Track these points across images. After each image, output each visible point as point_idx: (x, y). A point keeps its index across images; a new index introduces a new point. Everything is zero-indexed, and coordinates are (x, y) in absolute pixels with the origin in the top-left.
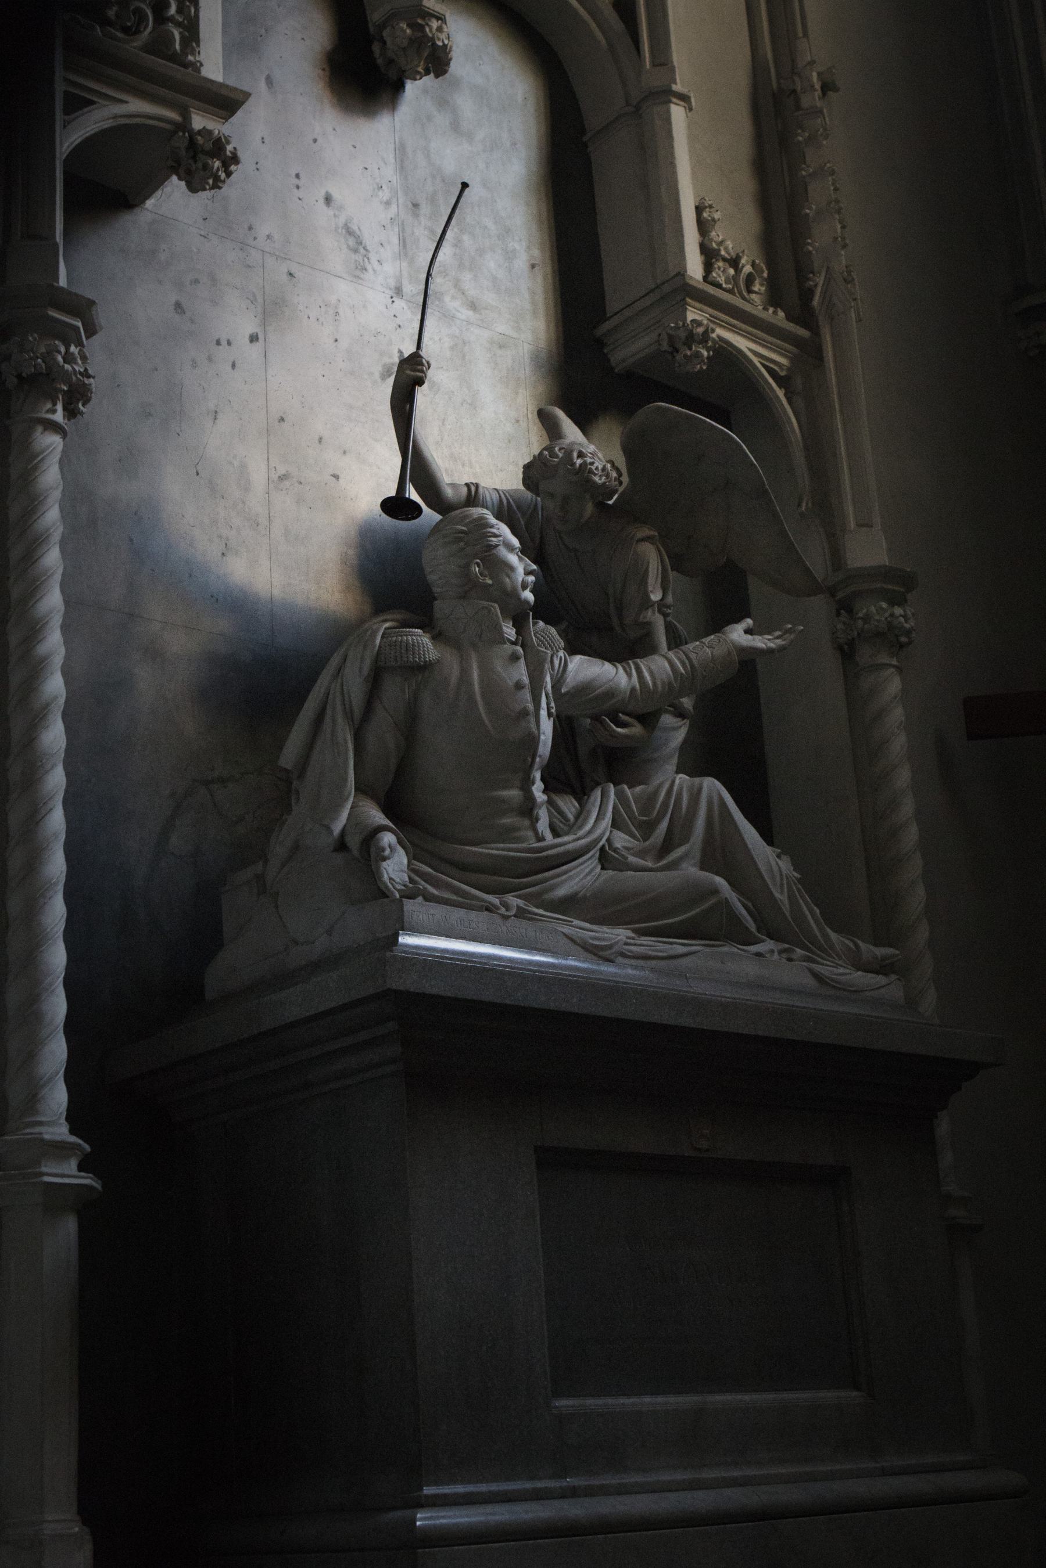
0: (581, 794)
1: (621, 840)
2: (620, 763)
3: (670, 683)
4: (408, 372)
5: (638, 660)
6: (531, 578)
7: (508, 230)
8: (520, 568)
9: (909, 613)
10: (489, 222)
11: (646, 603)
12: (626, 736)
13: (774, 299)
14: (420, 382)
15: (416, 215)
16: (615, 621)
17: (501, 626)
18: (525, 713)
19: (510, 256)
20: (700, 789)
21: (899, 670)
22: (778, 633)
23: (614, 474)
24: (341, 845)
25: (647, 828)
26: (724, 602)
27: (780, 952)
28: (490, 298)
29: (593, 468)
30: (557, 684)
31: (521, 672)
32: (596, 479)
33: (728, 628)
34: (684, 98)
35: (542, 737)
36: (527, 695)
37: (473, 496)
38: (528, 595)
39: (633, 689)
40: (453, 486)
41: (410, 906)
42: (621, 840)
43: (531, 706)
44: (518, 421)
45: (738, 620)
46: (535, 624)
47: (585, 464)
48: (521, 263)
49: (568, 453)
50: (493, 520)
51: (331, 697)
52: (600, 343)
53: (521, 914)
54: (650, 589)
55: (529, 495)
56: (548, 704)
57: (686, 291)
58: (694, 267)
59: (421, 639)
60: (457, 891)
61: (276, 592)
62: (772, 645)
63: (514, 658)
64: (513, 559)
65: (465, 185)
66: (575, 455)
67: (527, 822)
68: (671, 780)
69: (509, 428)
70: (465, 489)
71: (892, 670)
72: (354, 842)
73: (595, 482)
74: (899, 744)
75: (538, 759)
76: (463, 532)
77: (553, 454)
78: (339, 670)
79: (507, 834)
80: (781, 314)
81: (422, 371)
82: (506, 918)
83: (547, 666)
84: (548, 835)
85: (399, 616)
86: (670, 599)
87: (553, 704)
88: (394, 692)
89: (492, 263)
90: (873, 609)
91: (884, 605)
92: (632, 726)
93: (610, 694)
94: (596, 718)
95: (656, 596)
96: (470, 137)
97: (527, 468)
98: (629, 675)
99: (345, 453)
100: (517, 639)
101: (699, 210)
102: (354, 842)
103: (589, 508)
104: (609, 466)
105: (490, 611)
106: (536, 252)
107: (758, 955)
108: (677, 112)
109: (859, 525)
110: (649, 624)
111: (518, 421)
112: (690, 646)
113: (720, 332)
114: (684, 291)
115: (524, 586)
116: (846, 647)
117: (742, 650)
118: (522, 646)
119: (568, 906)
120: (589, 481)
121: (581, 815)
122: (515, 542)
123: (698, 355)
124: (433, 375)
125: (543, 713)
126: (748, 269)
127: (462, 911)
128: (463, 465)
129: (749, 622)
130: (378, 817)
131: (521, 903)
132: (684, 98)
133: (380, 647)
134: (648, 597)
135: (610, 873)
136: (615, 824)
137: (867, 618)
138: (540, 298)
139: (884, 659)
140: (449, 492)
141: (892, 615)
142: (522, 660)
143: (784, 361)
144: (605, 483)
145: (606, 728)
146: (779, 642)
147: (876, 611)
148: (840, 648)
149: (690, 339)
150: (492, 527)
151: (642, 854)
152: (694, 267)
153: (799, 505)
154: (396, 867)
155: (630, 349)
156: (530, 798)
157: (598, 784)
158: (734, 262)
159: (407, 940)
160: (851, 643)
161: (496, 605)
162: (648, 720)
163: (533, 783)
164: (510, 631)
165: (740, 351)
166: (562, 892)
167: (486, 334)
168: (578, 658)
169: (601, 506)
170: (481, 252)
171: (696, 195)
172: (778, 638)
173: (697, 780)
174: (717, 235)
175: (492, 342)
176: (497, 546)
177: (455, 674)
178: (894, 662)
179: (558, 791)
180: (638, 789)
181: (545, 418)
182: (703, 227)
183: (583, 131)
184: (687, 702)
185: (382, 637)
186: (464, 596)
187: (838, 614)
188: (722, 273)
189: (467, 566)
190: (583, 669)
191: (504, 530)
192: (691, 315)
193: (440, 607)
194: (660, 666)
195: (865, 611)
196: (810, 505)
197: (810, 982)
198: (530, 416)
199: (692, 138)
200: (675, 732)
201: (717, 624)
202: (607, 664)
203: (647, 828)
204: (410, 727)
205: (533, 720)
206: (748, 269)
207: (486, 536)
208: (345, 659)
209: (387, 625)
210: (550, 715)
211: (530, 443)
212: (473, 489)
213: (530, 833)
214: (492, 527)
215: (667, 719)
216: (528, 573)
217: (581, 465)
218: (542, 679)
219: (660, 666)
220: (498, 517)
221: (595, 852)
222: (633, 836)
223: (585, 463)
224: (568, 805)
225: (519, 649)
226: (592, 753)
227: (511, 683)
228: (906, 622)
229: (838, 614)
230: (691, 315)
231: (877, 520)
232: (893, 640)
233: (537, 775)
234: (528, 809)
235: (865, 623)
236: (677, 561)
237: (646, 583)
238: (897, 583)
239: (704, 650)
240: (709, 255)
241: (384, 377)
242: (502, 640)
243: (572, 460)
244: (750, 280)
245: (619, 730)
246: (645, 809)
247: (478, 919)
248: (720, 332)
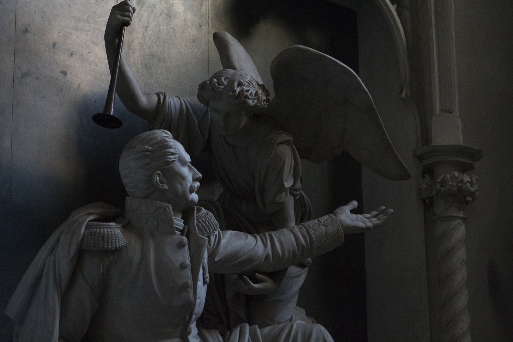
3: (294, 252)
4: (119, 17)
5: (273, 233)
6: (197, 184)
9: (474, 179)
11: (281, 188)
12: (260, 289)
14: (127, 24)
17: (173, 222)
18: (185, 286)
20: (311, 334)
21: (464, 220)
22: (375, 213)
23: (264, 97)
29: (248, 94)
32: (250, 102)
33: (338, 210)
35: (198, 301)
36: (188, 273)
38: (195, 197)
39: (267, 256)
43: (190, 282)
44: (201, 26)
45: (346, 203)
46: (199, 211)
47: (242, 91)
49: (231, 82)
51: (46, 267)
54: (285, 178)
56: (204, 275)
62: (369, 224)
63: (181, 245)
66: (236, 84)
69: (194, 32)
70: (156, 98)
71: (459, 221)
73: (249, 105)
74: (461, 276)
75: (194, 317)
76: (148, 151)
77: (220, 83)
78: (53, 250)
81: (129, 16)
85: (98, 211)
86: (299, 185)
87: (207, 275)
88: (92, 268)
90: (448, 176)
91: (456, 174)
92: (266, 282)
93: (250, 260)
94: (240, 276)
95: (288, 184)
97: (202, 86)
98: (265, 245)
99: (72, 55)
100: (184, 228)
103: (244, 121)
104: (260, 92)
105: (165, 210)
109: (442, 110)
110: (283, 203)
111: (201, 26)
115: (191, 191)
116: (427, 201)
118: (187, 236)
120: (245, 104)
122: (187, 157)
124: (136, 20)
128: (159, 61)
129: (355, 203)
133: (84, 235)
134: (283, 185)
137: (443, 183)
139: (454, 212)
140: (143, 100)
141: (462, 181)
142: (187, 247)
144: (256, 105)
146: (375, 221)
147: (450, 177)
148: (424, 200)
150: (171, 147)
153: (401, 92)
157: (239, 321)
160: (431, 198)
161: (170, 206)
162: (277, 275)
163: (189, 334)
164: (179, 222)
168: (229, 234)
172: (375, 216)
176: (173, 161)
177: (137, 254)
178: (461, 215)
180: (267, 330)
181: (219, 41)
185: (86, 228)
187: (423, 177)
189: (151, 176)
191: (179, 148)
194: (288, 238)
195: (442, 177)
196: (409, 93)
198: (210, 22)
200: (298, 278)
201: (333, 206)
202: (249, 236)
204: (102, 294)
205: (191, 291)
207: (166, 154)
208: (58, 241)
209: (91, 218)
210: (204, 282)
212: (162, 98)
214: (171, 147)
216: (195, 180)
217: (239, 92)
219: (288, 238)
223: (242, 90)
225: (185, 239)
227: (177, 264)
228: (471, 186)
229: (423, 177)
231: (456, 108)
232: (461, 198)
235: (442, 186)
237: (282, 175)
238: (466, 158)
239: (320, 226)
242: (171, 230)
243: (234, 88)
245: (255, 285)
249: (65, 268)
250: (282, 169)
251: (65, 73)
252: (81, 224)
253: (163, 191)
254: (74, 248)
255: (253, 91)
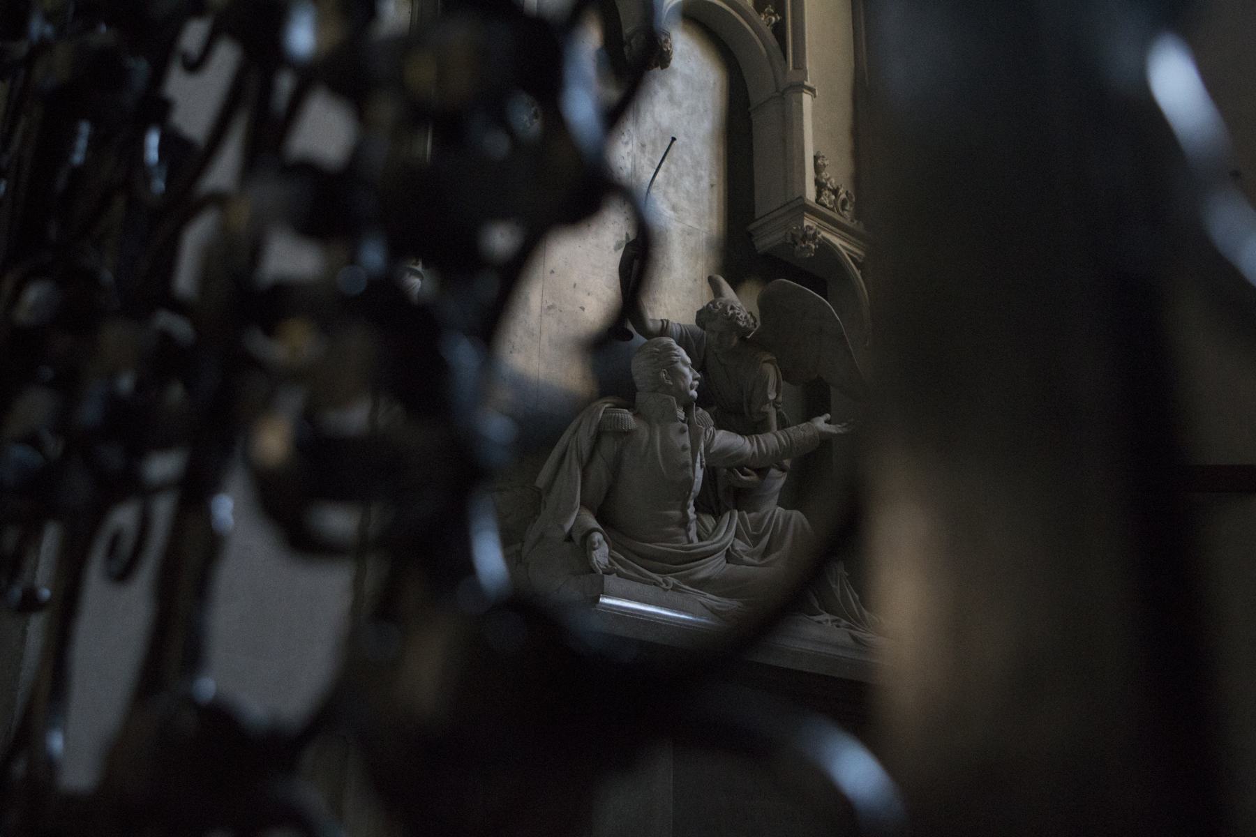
0: (717, 515)
1: (740, 546)
2: (743, 498)
6: (696, 383)
7: (698, 163)
8: (690, 375)
10: (687, 158)
11: (766, 400)
13: (858, 215)
15: (643, 152)
16: (746, 409)
18: (686, 465)
19: (698, 179)
24: (569, 538)
25: (756, 539)
26: (815, 403)
27: (833, 621)
28: (684, 204)
30: (707, 448)
31: (686, 440)
33: (815, 419)
34: (812, 90)
36: (689, 452)
37: (664, 330)
38: (694, 393)
40: (654, 320)
41: (610, 581)
42: (740, 546)
43: (690, 462)
45: (820, 414)
48: (705, 183)
49: (725, 306)
50: (676, 346)
52: (750, 235)
53: (675, 588)
55: (699, 329)
57: (804, 208)
58: (810, 193)
59: (627, 416)
60: (637, 571)
61: (541, 377)
63: (682, 431)
64: (686, 370)
65: (674, 139)
67: (683, 531)
68: (772, 510)
69: (690, 284)
72: (577, 536)
77: (715, 307)
78: (575, 431)
79: (669, 538)
80: (861, 224)
82: (666, 590)
83: (703, 436)
84: (695, 539)
88: (609, 447)
89: (687, 183)
93: (739, 455)
94: (730, 470)
95: (772, 397)
96: (679, 105)
97: (699, 313)
101: (816, 158)
102: (577, 536)
103: (735, 340)
106: (715, 177)
107: (819, 622)
108: (807, 98)
112: (791, 429)
113: (823, 233)
114: (802, 208)
115: (692, 387)
117: (822, 433)
119: (704, 584)
121: (716, 528)
122: (688, 360)
123: (809, 247)
125: (698, 465)
126: (843, 196)
127: (639, 585)
129: (828, 416)
130: (593, 523)
131: (676, 581)
132: (812, 90)
135: (731, 565)
136: (737, 535)
138: (715, 205)
140: (651, 325)
143: (859, 252)
145: (736, 475)
149: (805, 237)
151: (751, 555)
152: (810, 193)
154: (601, 555)
155: (768, 240)
156: (686, 516)
157: (727, 509)
158: (835, 192)
159: (605, 600)
162: (762, 472)
164: (681, 414)
165: (835, 246)
166: (702, 575)
167: (680, 226)
168: (722, 432)
169: (743, 339)
170: (681, 175)
171: (814, 149)
173: (789, 512)
174: (826, 174)
175: (683, 231)
177: (645, 437)
179: (704, 512)
180: (753, 514)
181: (712, 281)
182: (818, 169)
183: (749, 105)
184: (787, 463)
186: (654, 391)
188: (827, 198)
190: (725, 439)
191: (682, 352)
192: (807, 222)
193: (639, 397)
194: (771, 440)
197: (848, 640)
199: (814, 114)
200: (778, 480)
201: (809, 416)
203: (756, 539)
204: (616, 469)
206: (843, 196)
207: (670, 356)
208: (580, 424)
211: (703, 297)
213: (685, 538)
215: (774, 472)
216: (695, 379)
218: (698, 445)
219: (771, 440)
220: (678, 344)
221: (724, 552)
222: (746, 543)
224: (709, 521)
226: (726, 491)
227: (679, 446)
230: (807, 222)
233: (691, 503)
234: (684, 523)
236: (786, 375)
239: (800, 431)
240: (820, 186)
241: (617, 248)
242: (676, 419)
244: (844, 203)
246: (756, 528)
247: (648, 590)
248: (823, 233)
249: (585, 446)
250: (767, 383)
251: (583, 309)
252: (599, 410)
253: (668, 387)
254: (593, 428)
255: (743, 314)
